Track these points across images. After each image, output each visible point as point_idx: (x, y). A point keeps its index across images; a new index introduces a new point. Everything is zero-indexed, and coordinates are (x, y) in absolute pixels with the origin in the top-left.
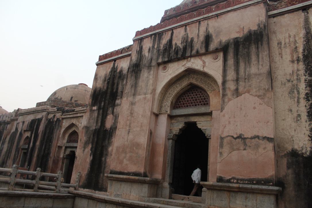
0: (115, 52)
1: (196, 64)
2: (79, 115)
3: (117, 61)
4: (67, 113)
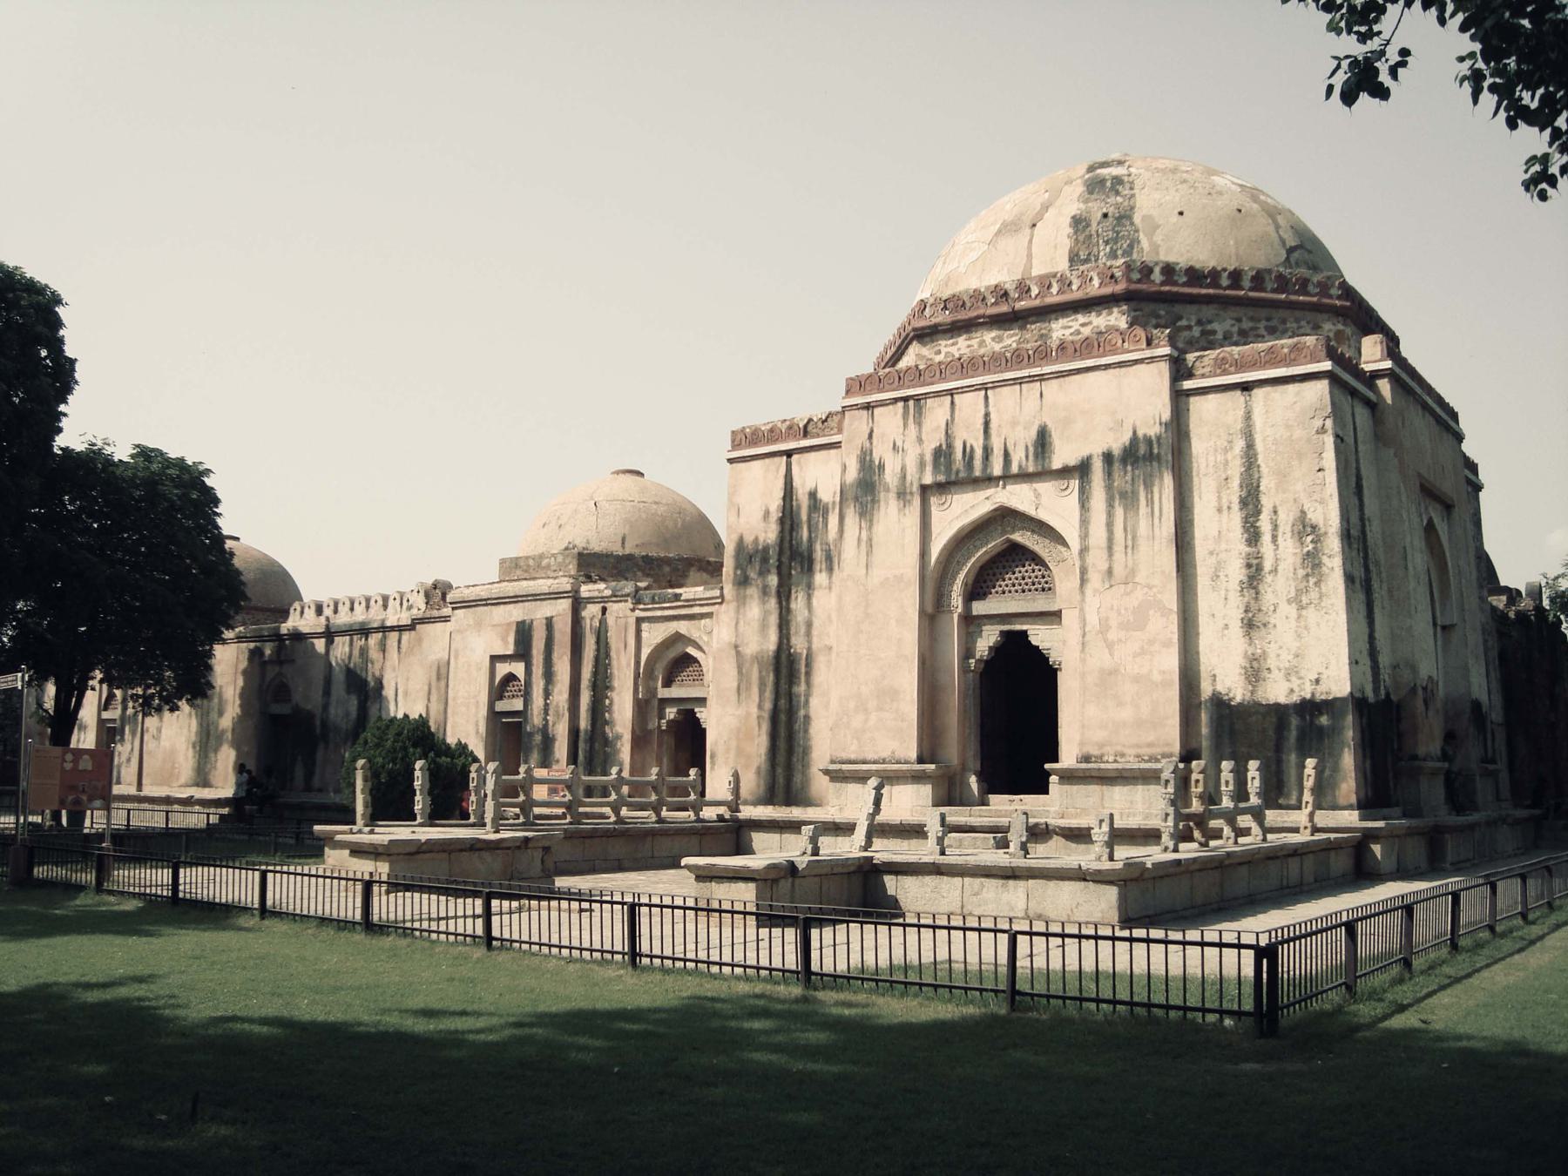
0: (784, 428)
1: (1018, 497)
2: (697, 610)
3: (795, 457)
4: (653, 602)
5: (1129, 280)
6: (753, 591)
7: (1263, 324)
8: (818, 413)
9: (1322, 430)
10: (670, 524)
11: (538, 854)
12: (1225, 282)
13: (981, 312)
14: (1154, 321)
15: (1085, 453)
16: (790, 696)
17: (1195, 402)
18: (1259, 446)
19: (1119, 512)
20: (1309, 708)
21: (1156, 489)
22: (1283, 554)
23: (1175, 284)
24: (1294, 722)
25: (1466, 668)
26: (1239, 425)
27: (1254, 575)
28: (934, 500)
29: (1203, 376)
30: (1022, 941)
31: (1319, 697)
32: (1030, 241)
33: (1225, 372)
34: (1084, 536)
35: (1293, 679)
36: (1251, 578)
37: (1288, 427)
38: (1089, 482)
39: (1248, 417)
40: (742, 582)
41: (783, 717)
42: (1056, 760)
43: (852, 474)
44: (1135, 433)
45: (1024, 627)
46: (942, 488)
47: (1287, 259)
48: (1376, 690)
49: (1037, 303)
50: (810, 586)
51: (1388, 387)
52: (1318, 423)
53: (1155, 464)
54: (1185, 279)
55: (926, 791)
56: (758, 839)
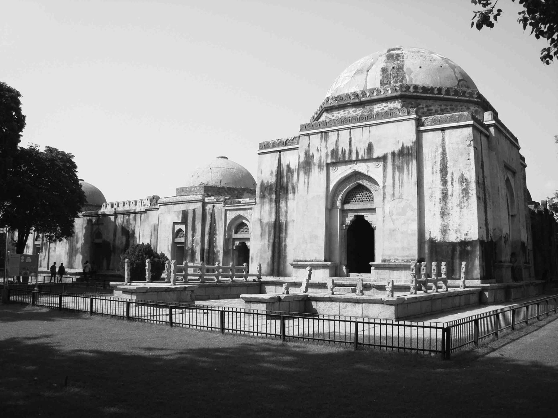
1: (361, 168)
2: (246, 207)
3: (282, 153)
4: (231, 204)
5: (402, 91)
6: (266, 200)
7: (449, 107)
8: (290, 137)
9: (470, 145)
10: (237, 176)
11: (189, 293)
12: (436, 92)
13: (349, 102)
14: (410, 106)
15: (385, 152)
16: (279, 238)
17: (425, 135)
18: (447, 151)
19: (397, 173)
20: (464, 244)
21: (410, 166)
22: (455, 189)
23: (418, 92)
24: (458, 248)
25: (519, 231)
26: (440, 143)
27: (445, 196)
28: (331, 168)
29: (427, 125)
30: (360, 325)
31: (467, 240)
32: (367, 77)
33: (435, 124)
34: (385, 182)
35: (458, 233)
36: (444, 197)
37: (457, 144)
38: (387, 163)
39: (443, 140)
40: (263, 197)
41: (277, 245)
42: (374, 261)
43: (302, 159)
44: (403, 145)
45: (363, 214)
46: (334, 164)
47: (458, 84)
48: (487, 238)
49: (369, 98)
50: (287, 199)
51: (493, 130)
52: (468, 143)
53: (410, 157)
54: (421, 91)
55: (327, 271)
56: (268, 288)
